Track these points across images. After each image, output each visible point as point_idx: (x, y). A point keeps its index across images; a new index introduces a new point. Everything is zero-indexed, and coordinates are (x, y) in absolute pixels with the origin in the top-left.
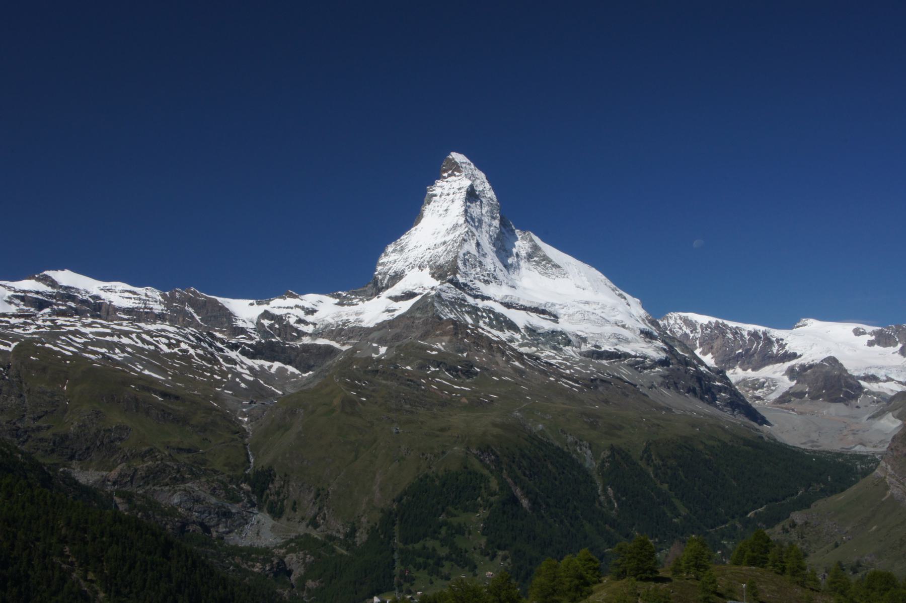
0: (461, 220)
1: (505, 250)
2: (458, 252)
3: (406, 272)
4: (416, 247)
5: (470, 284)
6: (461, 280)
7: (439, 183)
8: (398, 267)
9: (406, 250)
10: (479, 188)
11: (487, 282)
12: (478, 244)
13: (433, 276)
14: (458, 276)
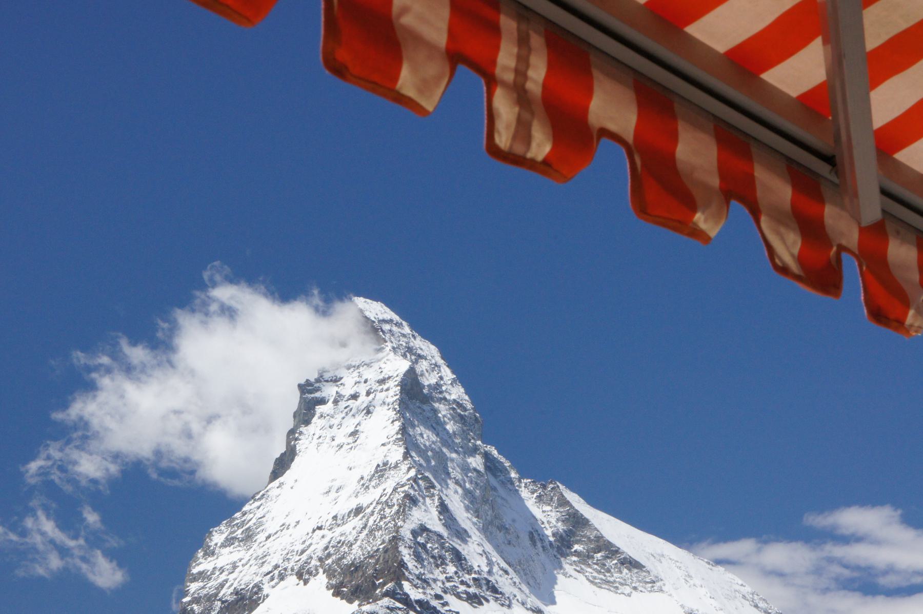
0: (396, 453)
1: (502, 528)
2: (397, 529)
3: (266, 589)
5: (435, 603)
6: (415, 594)
8: (245, 578)
9: (261, 537)
10: (429, 380)
12: (444, 509)
13: (337, 593)
14: (406, 586)
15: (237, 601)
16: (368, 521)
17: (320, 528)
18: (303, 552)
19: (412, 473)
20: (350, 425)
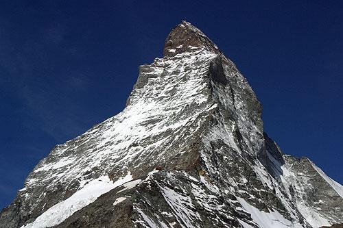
0: (202, 99)
4: (109, 143)
7: (161, 62)
11: (262, 207)
15: (56, 192)
16: (174, 138)
17: (135, 145)
18: (118, 160)
19: (215, 106)
20: (169, 87)
